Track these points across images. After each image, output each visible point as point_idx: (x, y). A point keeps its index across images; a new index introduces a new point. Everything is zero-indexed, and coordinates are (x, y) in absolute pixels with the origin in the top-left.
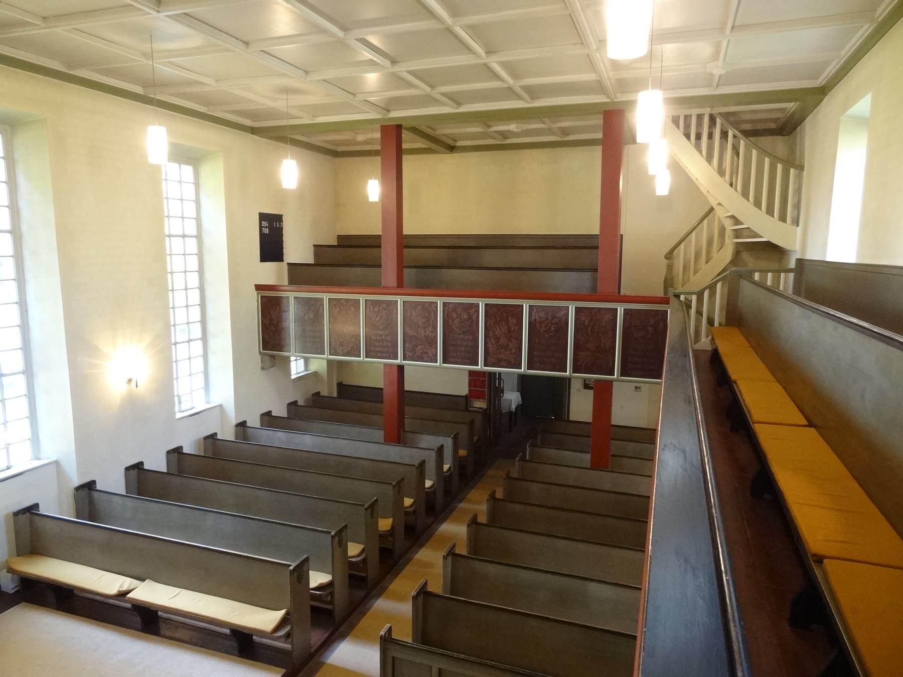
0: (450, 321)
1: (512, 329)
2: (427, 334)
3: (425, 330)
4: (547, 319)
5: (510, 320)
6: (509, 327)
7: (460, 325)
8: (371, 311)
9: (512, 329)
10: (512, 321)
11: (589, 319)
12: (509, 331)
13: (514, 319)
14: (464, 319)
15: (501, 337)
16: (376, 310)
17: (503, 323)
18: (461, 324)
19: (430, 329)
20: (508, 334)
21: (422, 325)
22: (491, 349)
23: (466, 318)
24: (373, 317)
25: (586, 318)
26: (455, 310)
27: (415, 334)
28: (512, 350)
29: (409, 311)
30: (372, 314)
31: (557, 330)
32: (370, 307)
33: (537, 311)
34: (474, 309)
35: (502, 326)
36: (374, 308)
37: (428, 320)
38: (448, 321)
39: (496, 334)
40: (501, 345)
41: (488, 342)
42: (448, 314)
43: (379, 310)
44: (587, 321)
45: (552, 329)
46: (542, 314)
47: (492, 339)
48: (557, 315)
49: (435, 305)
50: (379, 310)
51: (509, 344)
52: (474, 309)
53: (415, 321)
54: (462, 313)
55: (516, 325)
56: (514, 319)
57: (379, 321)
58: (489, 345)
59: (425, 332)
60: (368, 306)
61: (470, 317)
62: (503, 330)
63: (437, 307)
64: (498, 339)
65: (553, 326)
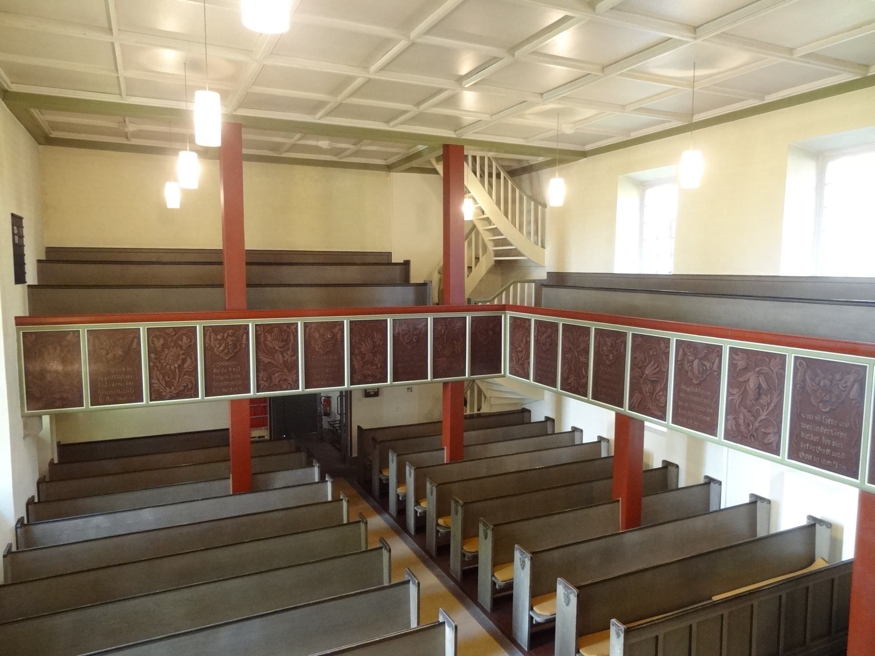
0: (312, 343)
8: (212, 340)
16: (219, 337)
24: (216, 346)
27: (271, 361)
29: (263, 335)
30: (214, 343)
32: (210, 336)
35: (368, 343)
36: (216, 335)
42: (309, 335)
53: (271, 345)
56: (379, 334)
57: (223, 351)
60: (208, 334)
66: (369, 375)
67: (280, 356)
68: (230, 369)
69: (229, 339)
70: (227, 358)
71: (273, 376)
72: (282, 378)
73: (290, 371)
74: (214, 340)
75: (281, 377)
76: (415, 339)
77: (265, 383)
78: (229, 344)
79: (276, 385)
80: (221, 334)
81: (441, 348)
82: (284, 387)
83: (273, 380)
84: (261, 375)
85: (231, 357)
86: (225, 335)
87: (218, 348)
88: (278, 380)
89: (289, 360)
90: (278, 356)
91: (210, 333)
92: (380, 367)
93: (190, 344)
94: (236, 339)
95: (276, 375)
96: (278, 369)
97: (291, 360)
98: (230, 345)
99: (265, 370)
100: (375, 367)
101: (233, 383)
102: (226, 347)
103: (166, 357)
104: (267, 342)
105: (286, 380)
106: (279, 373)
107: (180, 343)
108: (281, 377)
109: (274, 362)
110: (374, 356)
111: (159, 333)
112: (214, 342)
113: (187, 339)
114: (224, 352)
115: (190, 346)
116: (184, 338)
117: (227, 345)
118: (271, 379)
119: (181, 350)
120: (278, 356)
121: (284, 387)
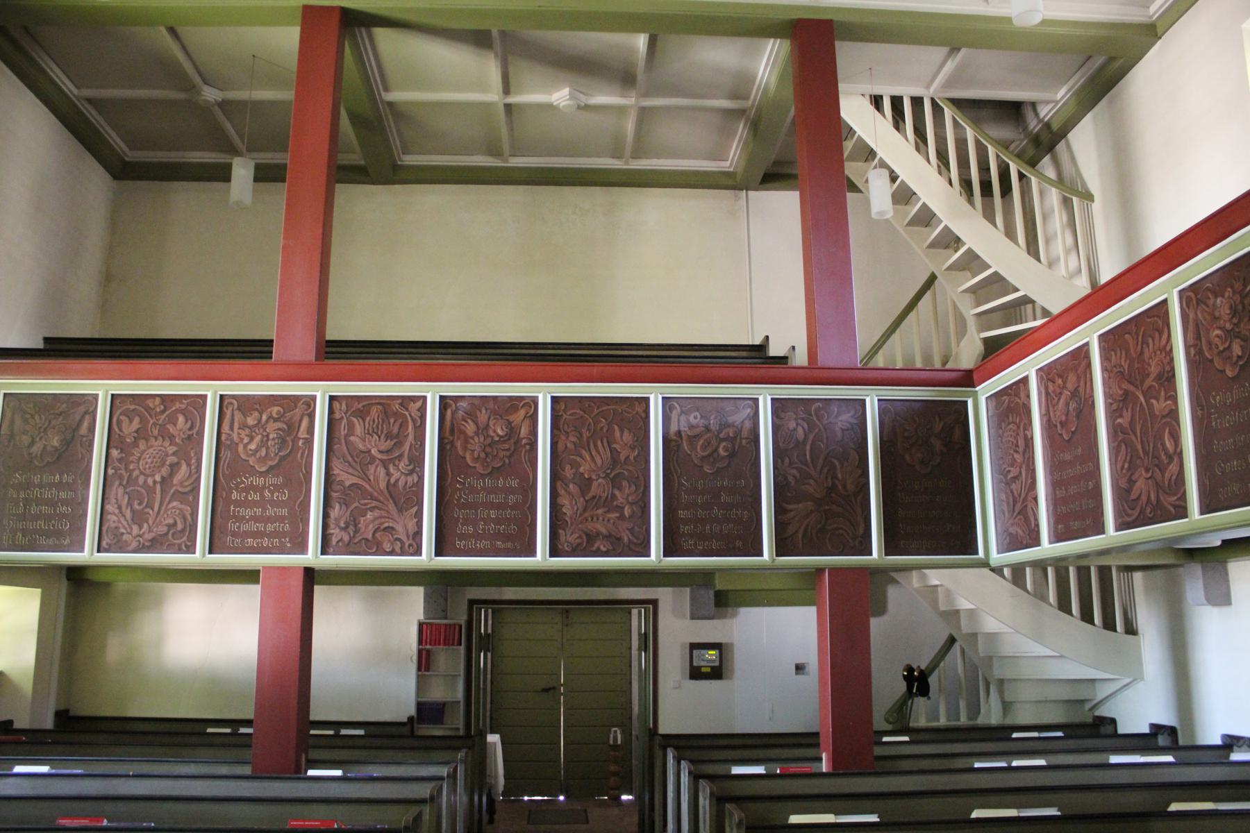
1: (622, 458)
2: (393, 480)
3: (386, 468)
4: (707, 429)
5: (617, 434)
6: (615, 454)
7: (487, 454)
8: (236, 425)
9: (622, 458)
10: (623, 438)
11: (806, 426)
12: (615, 461)
13: (626, 433)
14: (497, 439)
15: (594, 477)
16: (251, 421)
17: (599, 443)
18: (488, 450)
19: (402, 464)
20: (612, 470)
21: (380, 456)
22: (567, 510)
23: (500, 433)
24: (242, 440)
25: (797, 424)
26: (471, 415)
27: (360, 482)
28: (623, 508)
30: (239, 434)
31: (732, 455)
32: (233, 415)
33: (682, 412)
34: (522, 413)
36: (245, 415)
37: (399, 444)
38: (452, 443)
39: (582, 470)
40: (594, 497)
41: (562, 492)
43: (260, 421)
44: (800, 430)
45: (722, 452)
46: (695, 419)
47: (571, 486)
48: (731, 419)
49: (419, 404)
50: (260, 421)
51: (613, 496)
52: (522, 413)
54: (491, 424)
55: (632, 448)
57: (256, 451)
58: (564, 500)
59: (389, 474)
61: (512, 431)
62: (599, 461)
63: (423, 410)
64: (585, 484)
65: (721, 446)
66: (598, 533)
67: (381, 471)
68: (267, 493)
69: (272, 426)
70: (263, 469)
71: (362, 519)
72: (382, 524)
73: (401, 510)
74: (239, 428)
75: (377, 522)
76: (726, 449)
77: (343, 533)
78: (271, 436)
79: (367, 540)
80: (256, 414)
81: (795, 477)
82: (387, 547)
83: (362, 525)
84: (335, 512)
85: (271, 468)
86: (264, 417)
87: (246, 446)
88: (371, 528)
89: (401, 484)
90: (375, 471)
91: (233, 410)
92: (631, 517)
93: (191, 433)
94: (285, 427)
95: (369, 515)
96: (374, 503)
97: (406, 483)
98: (274, 439)
99: (345, 503)
100: (617, 515)
101: (270, 528)
102: (263, 443)
103: (140, 458)
104: (352, 438)
105: (390, 529)
106: (377, 513)
107: (170, 428)
108: (377, 522)
109: (364, 484)
110: (613, 487)
111: (132, 407)
112: (240, 431)
113: (186, 422)
114: (258, 455)
115: (190, 437)
116: (181, 419)
117: (265, 439)
118: (356, 526)
119: (170, 445)
120: (375, 471)
121: (387, 547)
